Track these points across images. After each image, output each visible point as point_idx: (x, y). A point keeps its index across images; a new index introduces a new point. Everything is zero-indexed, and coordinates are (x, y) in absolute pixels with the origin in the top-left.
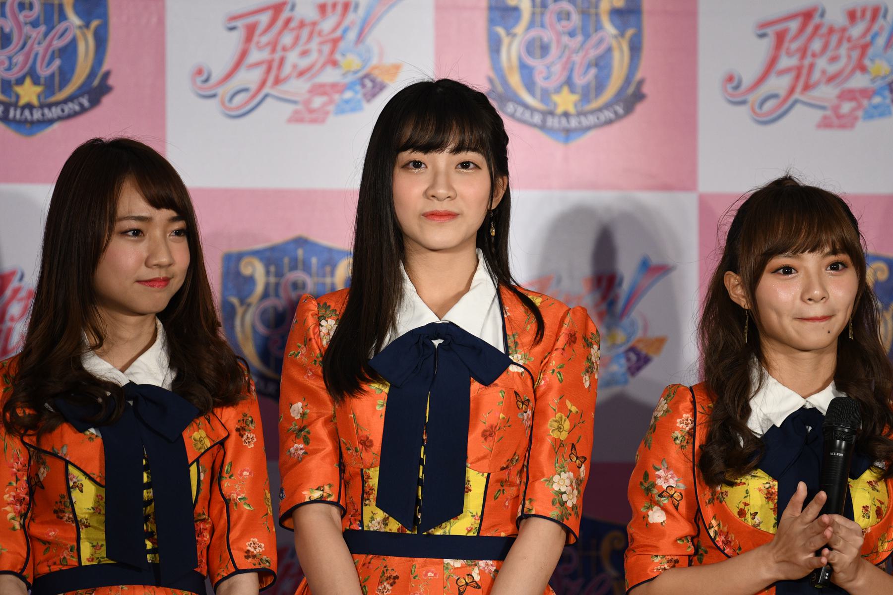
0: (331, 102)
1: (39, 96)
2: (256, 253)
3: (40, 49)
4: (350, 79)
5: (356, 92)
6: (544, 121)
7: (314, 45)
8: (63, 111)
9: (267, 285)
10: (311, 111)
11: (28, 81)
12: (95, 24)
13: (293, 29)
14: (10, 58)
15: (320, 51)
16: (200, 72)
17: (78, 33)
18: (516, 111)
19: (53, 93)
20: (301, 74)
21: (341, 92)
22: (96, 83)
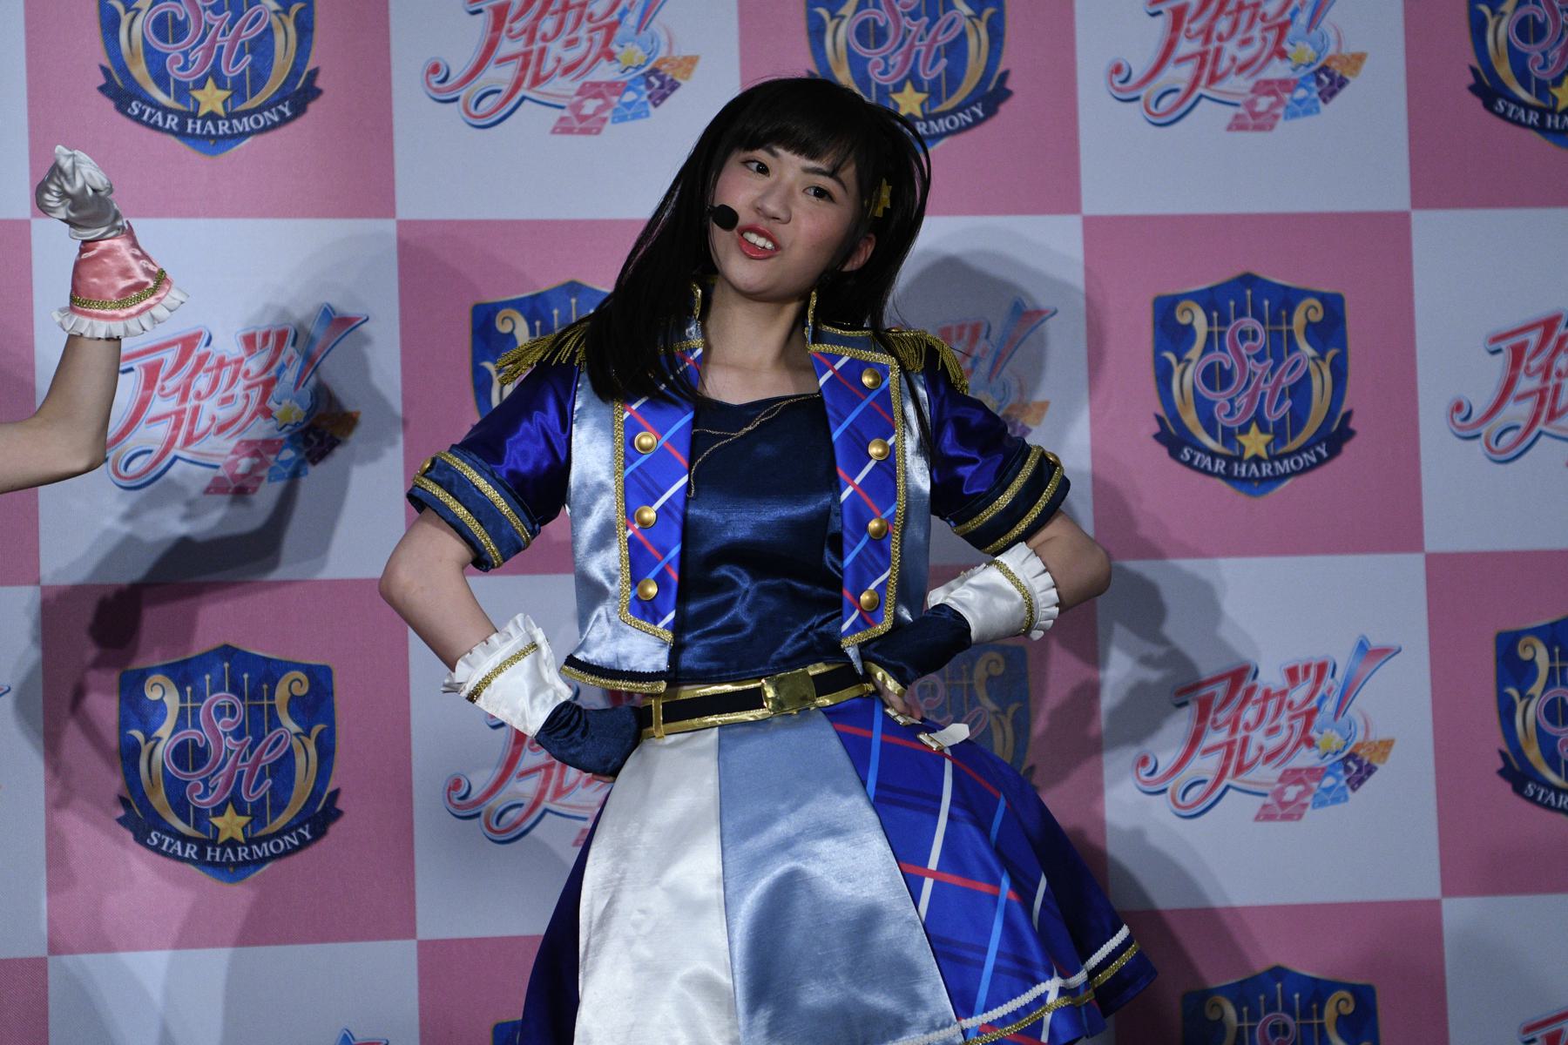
0: (1280, 102)
1: (922, 105)
2: (1195, 296)
3: (922, 47)
4: (1302, 72)
5: (1310, 90)
6: (1542, 120)
7: (1256, 32)
8: (952, 123)
9: (1210, 335)
10: (1255, 115)
11: (909, 87)
12: (988, 12)
13: (1230, 13)
14: (885, 59)
15: (1264, 39)
16: (1117, 69)
17: (968, 23)
18: (1507, 109)
19: (940, 103)
20: (1241, 69)
21: (1291, 91)
22: (991, 87)
